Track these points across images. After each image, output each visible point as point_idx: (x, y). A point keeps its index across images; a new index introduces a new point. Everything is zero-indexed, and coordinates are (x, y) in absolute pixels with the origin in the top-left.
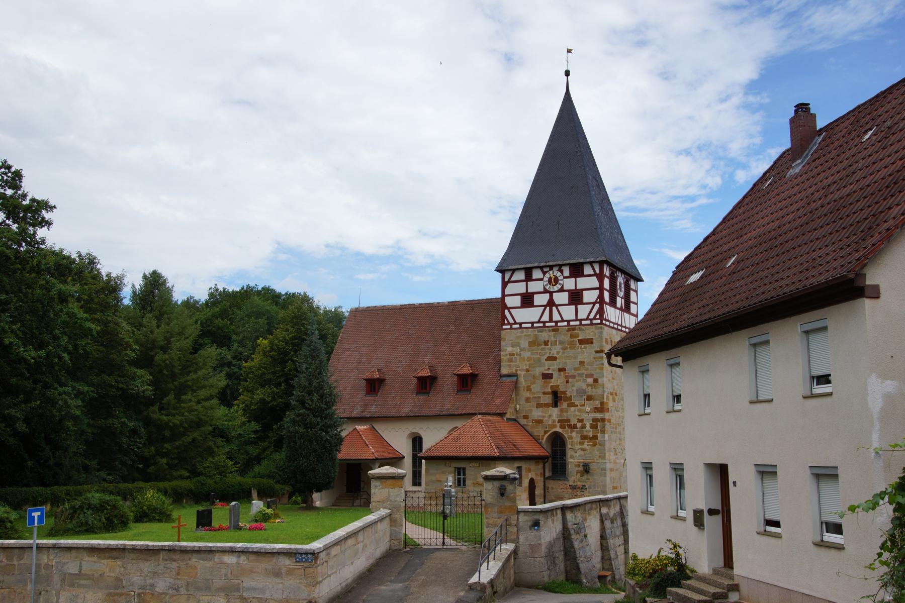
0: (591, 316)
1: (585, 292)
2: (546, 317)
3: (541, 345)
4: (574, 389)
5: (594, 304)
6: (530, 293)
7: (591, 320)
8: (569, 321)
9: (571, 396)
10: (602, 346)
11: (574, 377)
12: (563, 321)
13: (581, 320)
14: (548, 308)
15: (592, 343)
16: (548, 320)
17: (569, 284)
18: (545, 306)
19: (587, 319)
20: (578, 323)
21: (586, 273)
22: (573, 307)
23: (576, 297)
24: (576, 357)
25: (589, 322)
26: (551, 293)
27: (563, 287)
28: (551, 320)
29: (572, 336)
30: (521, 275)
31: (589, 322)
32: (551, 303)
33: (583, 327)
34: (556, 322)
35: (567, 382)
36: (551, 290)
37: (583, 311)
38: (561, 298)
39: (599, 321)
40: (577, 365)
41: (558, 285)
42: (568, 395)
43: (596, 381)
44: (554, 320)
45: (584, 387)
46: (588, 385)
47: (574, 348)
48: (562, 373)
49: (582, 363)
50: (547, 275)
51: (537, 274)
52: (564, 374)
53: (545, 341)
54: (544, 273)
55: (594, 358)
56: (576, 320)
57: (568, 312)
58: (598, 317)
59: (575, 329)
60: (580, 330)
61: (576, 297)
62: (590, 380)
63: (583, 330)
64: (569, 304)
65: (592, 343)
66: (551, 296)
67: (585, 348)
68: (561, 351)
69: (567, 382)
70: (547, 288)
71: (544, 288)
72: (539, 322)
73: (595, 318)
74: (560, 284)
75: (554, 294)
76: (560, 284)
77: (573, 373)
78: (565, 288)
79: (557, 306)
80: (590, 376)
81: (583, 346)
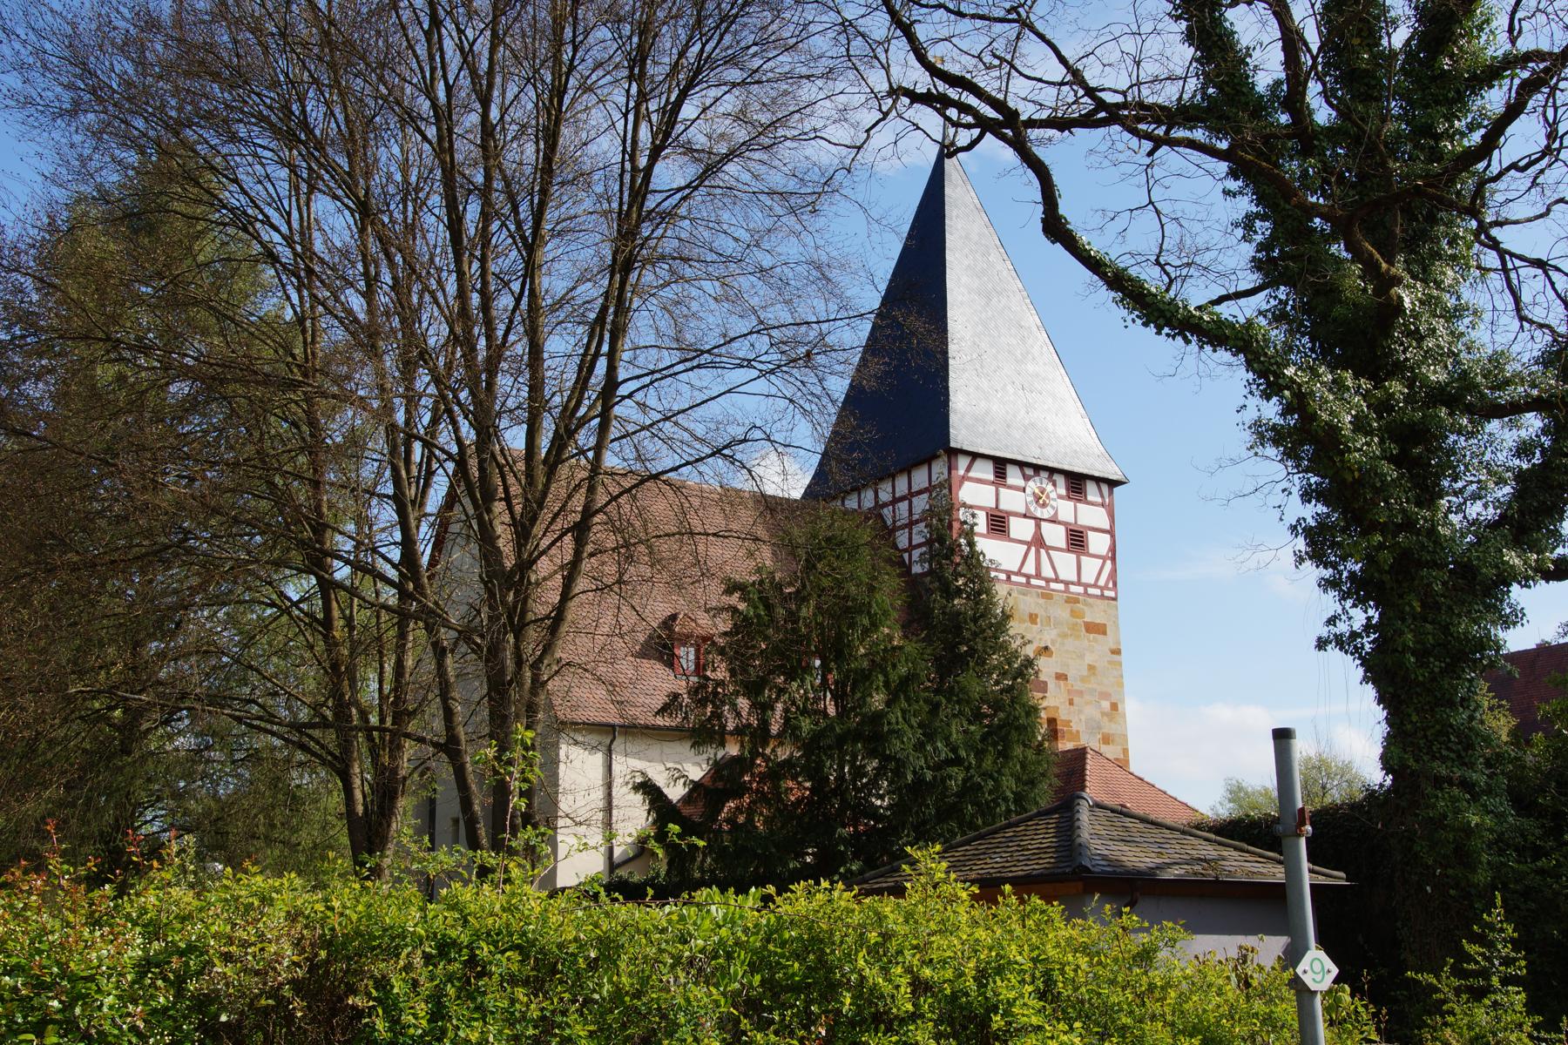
0: (1102, 582)
1: (1090, 534)
2: (1030, 568)
3: (1024, 621)
4: (1083, 718)
5: (1104, 558)
6: (1001, 511)
7: (1102, 589)
8: (1067, 583)
9: (1078, 732)
10: (1119, 643)
11: (1080, 693)
12: (1057, 580)
13: (1086, 586)
14: (1033, 549)
15: (1104, 633)
16: (1032, 572)
17: (1066, 510)
18: (1029, 544)
19: (1095, 586)
20: (1080, 589)
21: (1090, 498)
22: (1073, 556)
23: (1077, 540)
24: (1082, 657)
25: (1097, 592)
26: (1038, 520)
27: (1056, 513)
28: (1038, 576)
29: (1073, 613)
30: (985, 471)
31: (1097, 592)
32: (1038, 542)
33: (1090, 600)
34: (1048, 581)
35: (1071, 703)
36: (1039, 513)
37: (1090, 567)
38: (1055, 536)
39: (1112, 594)
40: (1085, 673)
41: (1049, 508)
42: (1074, 729)
43: (1114, 707)
44: (1043, 575)
45: (1098, 716)
46: (1103, 714)
47: (1078, 637)
48: (1062, 683)
49: (1091, 668)
50: (1031, 483)
51: (1014, 476)
52: (1066, 685)
53: (1031, 615)
54: (1026, 478)
55: (1110, 662)
56: (1079, 583)
57: (1066, 564)
58: (1111, 585)
59: (1077, 601)
60: (1086, 604)
61: (1077, 540)
62: (1106, 705)
63: (1090, 606)
64: (1068, 550)
65: (1104, 633)
66: (1038, 527)
67: (1095, 640)
68: (1059, 640)
69: (1071, 703)
70: (1032, 509)
71: (1027, 508)
72: (1019, 573)
73: (1106, 587)
74: (1053, 507)
75: (1043, 524)
76: (1053, 507)
77: (1078, 686)
78: (1061, 518)
79: (1048, 548)
80: (1105, 695)
81: (1092, 636)
